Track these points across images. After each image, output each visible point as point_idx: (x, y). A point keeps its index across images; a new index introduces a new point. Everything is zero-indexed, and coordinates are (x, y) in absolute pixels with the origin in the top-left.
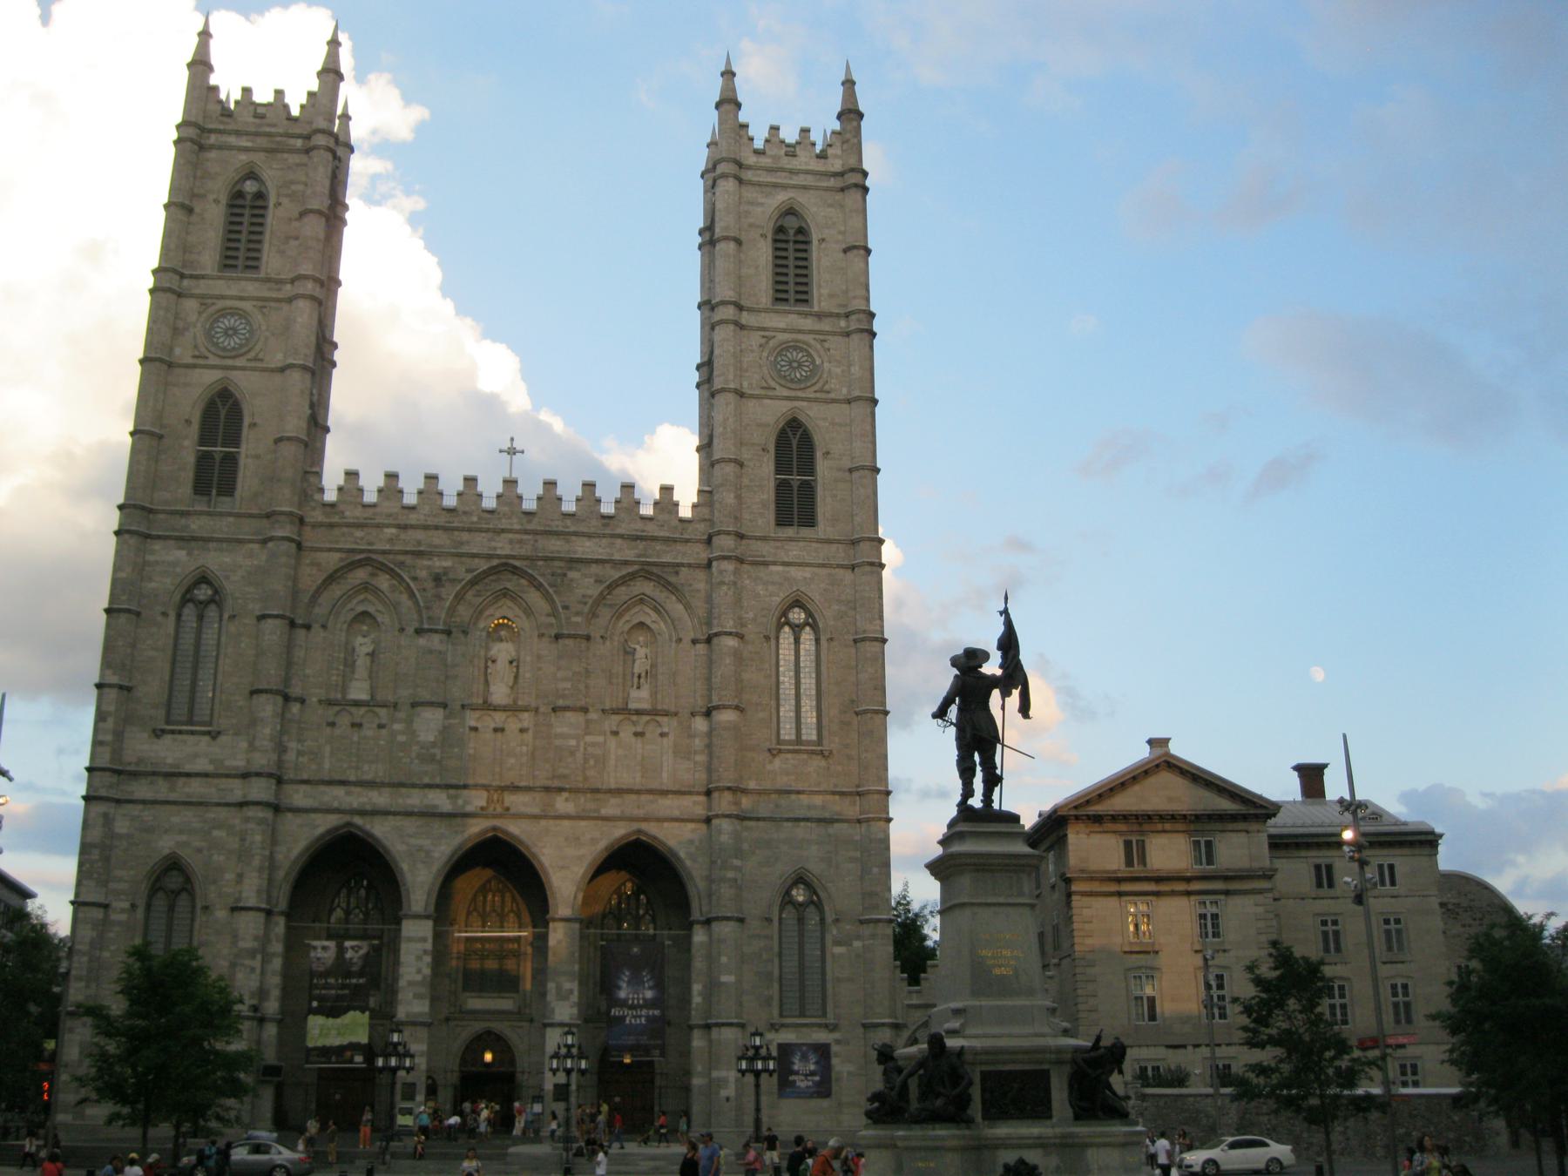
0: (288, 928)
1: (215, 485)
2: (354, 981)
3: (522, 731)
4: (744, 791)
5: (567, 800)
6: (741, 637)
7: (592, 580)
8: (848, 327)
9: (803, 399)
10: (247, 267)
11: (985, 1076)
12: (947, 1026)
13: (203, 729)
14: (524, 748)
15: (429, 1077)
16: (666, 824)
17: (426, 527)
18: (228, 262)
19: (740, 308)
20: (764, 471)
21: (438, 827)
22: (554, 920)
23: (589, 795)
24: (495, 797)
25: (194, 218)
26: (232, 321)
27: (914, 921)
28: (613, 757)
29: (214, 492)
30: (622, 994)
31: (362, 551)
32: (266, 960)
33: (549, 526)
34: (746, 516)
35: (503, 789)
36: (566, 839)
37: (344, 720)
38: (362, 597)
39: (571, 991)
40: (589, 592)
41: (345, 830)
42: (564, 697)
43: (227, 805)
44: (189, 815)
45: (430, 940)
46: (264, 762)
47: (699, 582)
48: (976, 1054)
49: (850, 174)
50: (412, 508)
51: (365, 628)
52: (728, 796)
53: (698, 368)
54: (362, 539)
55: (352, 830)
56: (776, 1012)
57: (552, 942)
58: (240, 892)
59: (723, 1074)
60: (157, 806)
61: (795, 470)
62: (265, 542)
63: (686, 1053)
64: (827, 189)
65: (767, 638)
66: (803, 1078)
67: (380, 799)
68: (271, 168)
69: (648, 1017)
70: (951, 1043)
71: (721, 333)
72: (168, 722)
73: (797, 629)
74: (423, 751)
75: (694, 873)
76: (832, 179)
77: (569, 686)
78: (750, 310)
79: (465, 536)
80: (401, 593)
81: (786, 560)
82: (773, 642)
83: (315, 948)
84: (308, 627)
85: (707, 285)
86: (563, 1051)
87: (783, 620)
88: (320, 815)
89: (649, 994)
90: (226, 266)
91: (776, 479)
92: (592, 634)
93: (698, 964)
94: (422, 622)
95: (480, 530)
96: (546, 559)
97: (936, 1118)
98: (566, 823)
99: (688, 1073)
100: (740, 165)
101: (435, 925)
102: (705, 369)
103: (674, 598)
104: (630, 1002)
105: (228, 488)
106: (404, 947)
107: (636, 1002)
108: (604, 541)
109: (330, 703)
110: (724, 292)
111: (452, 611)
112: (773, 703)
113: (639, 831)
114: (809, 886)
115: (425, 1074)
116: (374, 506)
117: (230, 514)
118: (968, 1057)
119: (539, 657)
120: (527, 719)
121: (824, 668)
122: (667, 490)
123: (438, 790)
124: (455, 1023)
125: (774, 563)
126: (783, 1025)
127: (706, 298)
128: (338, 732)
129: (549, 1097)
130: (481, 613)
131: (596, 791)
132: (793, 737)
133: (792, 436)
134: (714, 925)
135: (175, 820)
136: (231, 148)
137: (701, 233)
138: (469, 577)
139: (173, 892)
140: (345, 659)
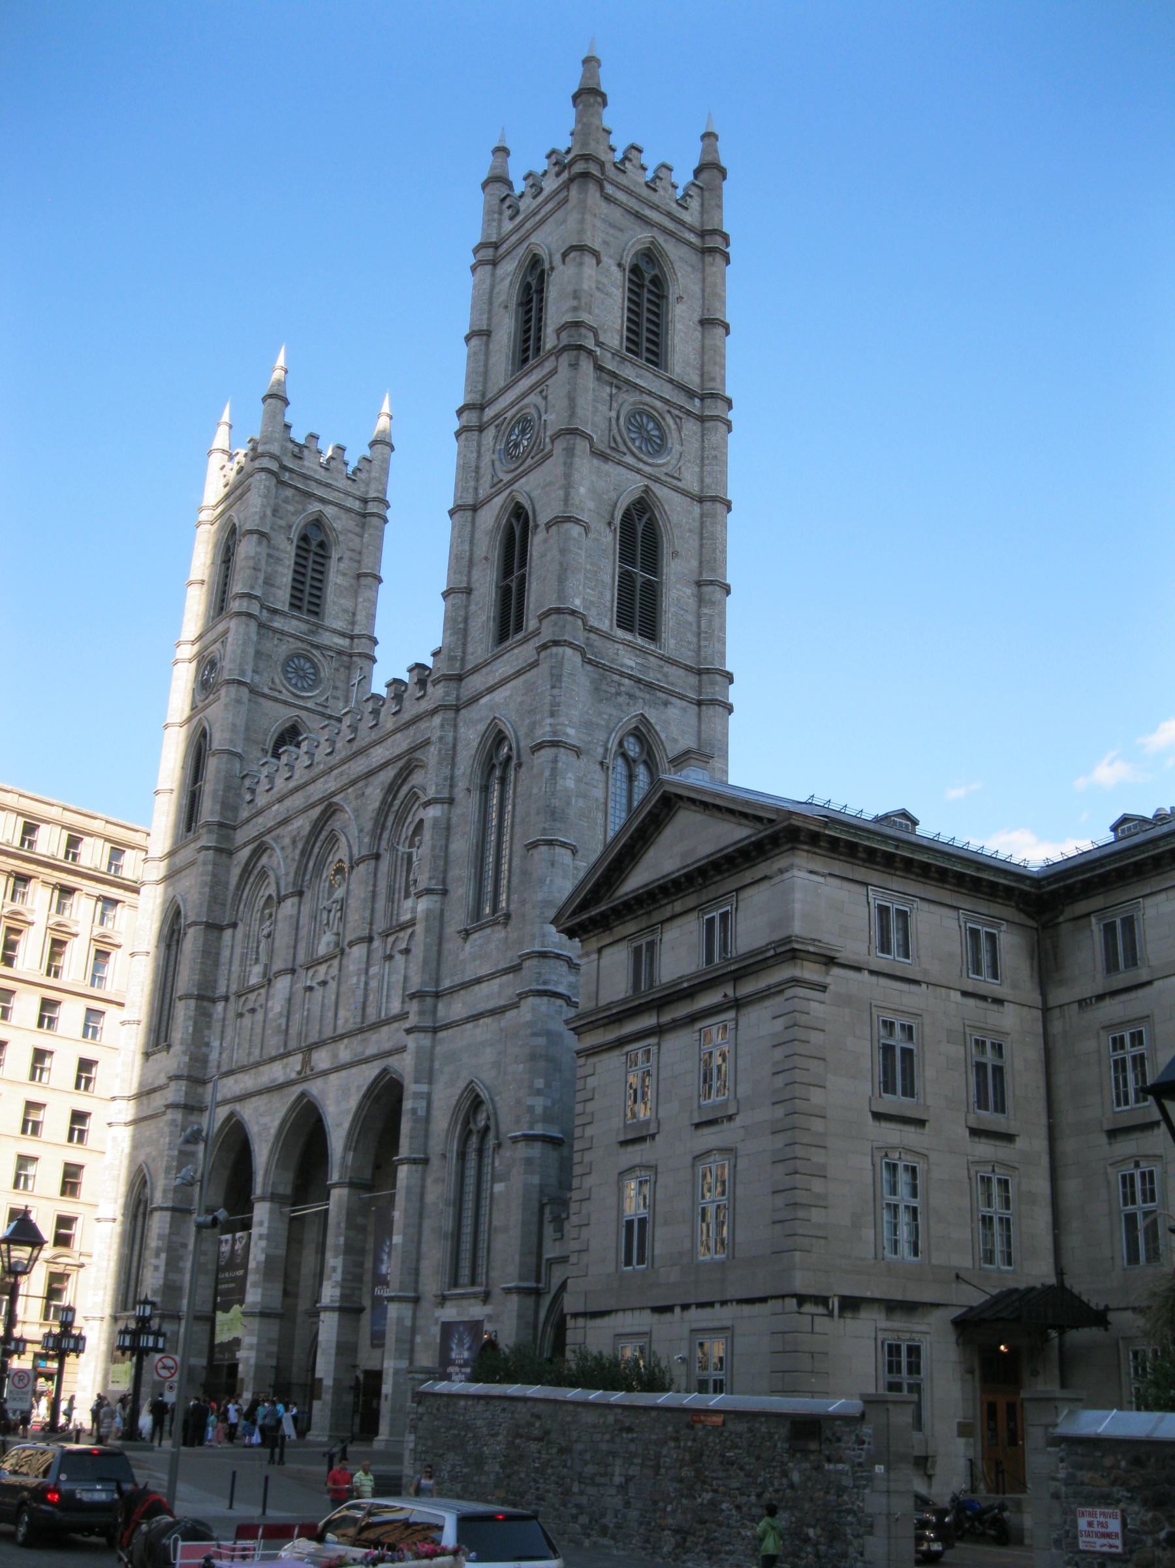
3: (333, 978)
4: (437, 995)
23: (359, 1036)
28: (385, 987)
39: (334, 1269)
45: (266, 1224)
46: (175, 1066)
65: (469, 790)
66: (457, 1369)
82: (476, 796)
84: (234, 925)
108: (390, 740)
111: (301, 870)
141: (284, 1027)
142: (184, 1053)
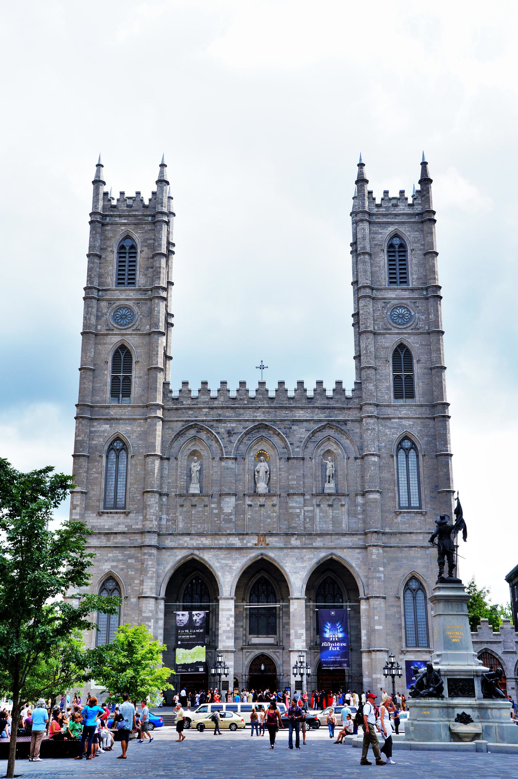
0: (166, 606)
1: (121, 392)
2: (198, 631)
3: (274, 505)
4: (384, 533)
5: (296, 539)
6: (379, 456)
8: (427, 294)
9: (406, 334)
10: (129, 283)
11: (449, 680)
12: (435, 661)
13: (122, 511)
14: (275, 514)
15: (235, 678)
16: (345, 550)
17: (222, 408)
18: (120, 282)
19: (372, 289)
20: (388, 371)
21: (235, 554)
22: (292, 599)
24: (262, 539)
25: (102, 261)
26: (124, 311)
27: (479, 596)
28: (318, 517)
29: (121, 395)
30: (327, 635)
31: (192, 421)
32: (156, 622)
33: (282, 404)
34: (379, 395)
35: (265, 535)
36: (297, 559)
37: (188, 504)
38: (193, 443)
39: (302, 634)
40: (303, 436)
41: (191, 557)
42: (293, 488)
43: (135, 547)
44: (117, 553)
45: (233, 610)
46: (151, 526)
47: (356, 428)
48: (445, 672)
49: (426, 213)
50: (216, 398)
51: (196, 458)
52: (375, 535)
53: (353, 316)
54: (192, 414)
55: (194, 557)
56: (404, 644)
57: (292, 610)
58: (143, 589)
59: (378, 676)
60: (102, 549)
61: (403, 370)
62: (146, 419)
63: (360, 665)
64: (414, 222)
67: (206, 541)
68: (137, 233)
69: (340, 647)
70: (435, 667)
71: (362, 303)
72: (105, 508)
73: (407, 451)
75: (360, 574)
76: (417, 217)
78: (377, 289)
79: (242, 411)
80: (212, 440)
81: (400, 416)
82: (395, 457)
83: (179, 615)
85: (355, 273)
86: (299, 665)
87: (400, 447)
88: (178, 550)
89: (341, 635)
90: (119, 283)
91: (394, 375)
92: (305, 457)
93: (364, 620)
94: (223, 455)
95: (249, 408)
96: (281, 421)
97: (430, 695)
98: (297, 550)
99: (361, 675)
100: (370, 214)
101: (236, 602)
102: (356, 316)
103: (345, 437)
104: (331, 639)
105: (127, 393)
106: (220, 613)
107: (334, 639)
109: (181, 496)
110: (362, 282)
111: (237, 448)
112: (396, 488)
113: (332, 554)
114: (417, 580)
115: (233, 677)
116: (197, 398)
117: (129, 406)
118: (442, 673)
119: (280, 468)
120: (275, 500)
121: (421, 470)
122: (339, 383)
123: (234, 536)
124: (246, 650)
125: (394, 418)
126: (408, 651)
127: (355, 280)
128: (185, 509)
129: (293, 687)
130: (251, 448)
131: (310, 534)
132: (407, 505)
133: (401, 353)
134: (371, 600)
135: (110, 555)
136: (117, 224)
137: (351, 245)
138: (245, 431)
139: (110, 590)
140: (187, 474)
141: (234, 520)
142: (156, 520)
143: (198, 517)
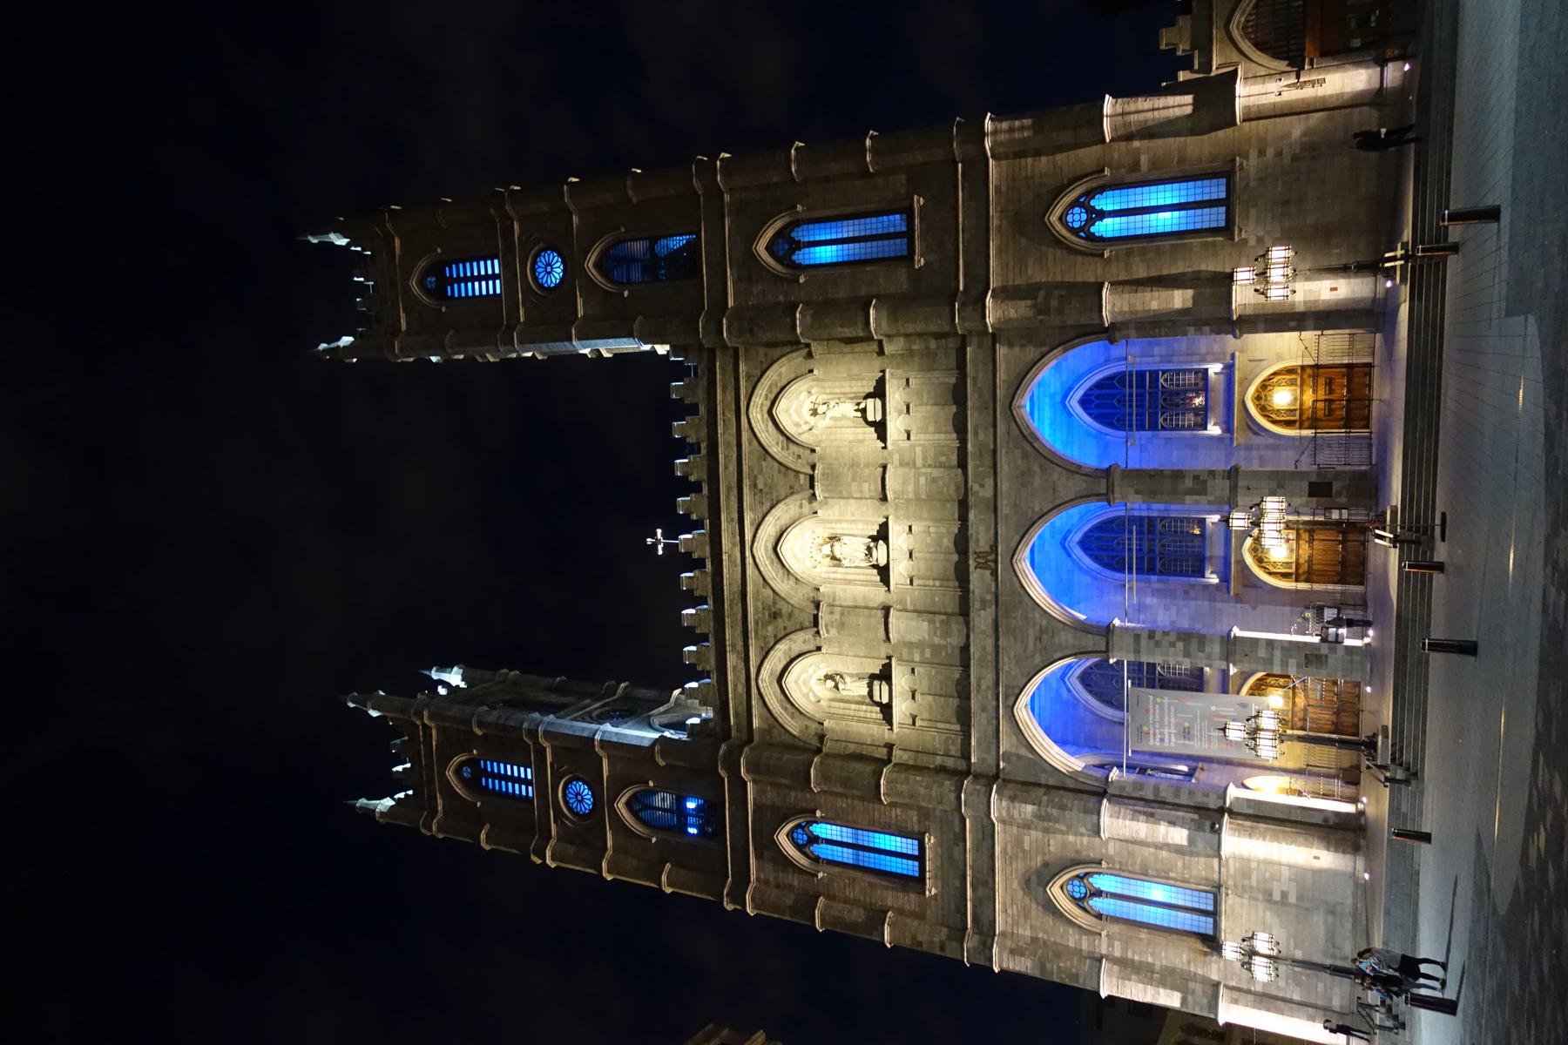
7: (764, 463)
14: (932, 530)
24: (981, 561)
36: (1024, 485)
74: (938, 634)
77: (867, 485)
98: (1004, 486)
132: (905, 240)
141: (944, 617)
143: (942, 689)
